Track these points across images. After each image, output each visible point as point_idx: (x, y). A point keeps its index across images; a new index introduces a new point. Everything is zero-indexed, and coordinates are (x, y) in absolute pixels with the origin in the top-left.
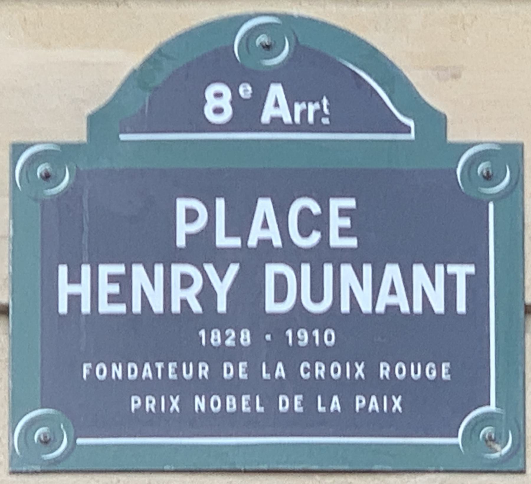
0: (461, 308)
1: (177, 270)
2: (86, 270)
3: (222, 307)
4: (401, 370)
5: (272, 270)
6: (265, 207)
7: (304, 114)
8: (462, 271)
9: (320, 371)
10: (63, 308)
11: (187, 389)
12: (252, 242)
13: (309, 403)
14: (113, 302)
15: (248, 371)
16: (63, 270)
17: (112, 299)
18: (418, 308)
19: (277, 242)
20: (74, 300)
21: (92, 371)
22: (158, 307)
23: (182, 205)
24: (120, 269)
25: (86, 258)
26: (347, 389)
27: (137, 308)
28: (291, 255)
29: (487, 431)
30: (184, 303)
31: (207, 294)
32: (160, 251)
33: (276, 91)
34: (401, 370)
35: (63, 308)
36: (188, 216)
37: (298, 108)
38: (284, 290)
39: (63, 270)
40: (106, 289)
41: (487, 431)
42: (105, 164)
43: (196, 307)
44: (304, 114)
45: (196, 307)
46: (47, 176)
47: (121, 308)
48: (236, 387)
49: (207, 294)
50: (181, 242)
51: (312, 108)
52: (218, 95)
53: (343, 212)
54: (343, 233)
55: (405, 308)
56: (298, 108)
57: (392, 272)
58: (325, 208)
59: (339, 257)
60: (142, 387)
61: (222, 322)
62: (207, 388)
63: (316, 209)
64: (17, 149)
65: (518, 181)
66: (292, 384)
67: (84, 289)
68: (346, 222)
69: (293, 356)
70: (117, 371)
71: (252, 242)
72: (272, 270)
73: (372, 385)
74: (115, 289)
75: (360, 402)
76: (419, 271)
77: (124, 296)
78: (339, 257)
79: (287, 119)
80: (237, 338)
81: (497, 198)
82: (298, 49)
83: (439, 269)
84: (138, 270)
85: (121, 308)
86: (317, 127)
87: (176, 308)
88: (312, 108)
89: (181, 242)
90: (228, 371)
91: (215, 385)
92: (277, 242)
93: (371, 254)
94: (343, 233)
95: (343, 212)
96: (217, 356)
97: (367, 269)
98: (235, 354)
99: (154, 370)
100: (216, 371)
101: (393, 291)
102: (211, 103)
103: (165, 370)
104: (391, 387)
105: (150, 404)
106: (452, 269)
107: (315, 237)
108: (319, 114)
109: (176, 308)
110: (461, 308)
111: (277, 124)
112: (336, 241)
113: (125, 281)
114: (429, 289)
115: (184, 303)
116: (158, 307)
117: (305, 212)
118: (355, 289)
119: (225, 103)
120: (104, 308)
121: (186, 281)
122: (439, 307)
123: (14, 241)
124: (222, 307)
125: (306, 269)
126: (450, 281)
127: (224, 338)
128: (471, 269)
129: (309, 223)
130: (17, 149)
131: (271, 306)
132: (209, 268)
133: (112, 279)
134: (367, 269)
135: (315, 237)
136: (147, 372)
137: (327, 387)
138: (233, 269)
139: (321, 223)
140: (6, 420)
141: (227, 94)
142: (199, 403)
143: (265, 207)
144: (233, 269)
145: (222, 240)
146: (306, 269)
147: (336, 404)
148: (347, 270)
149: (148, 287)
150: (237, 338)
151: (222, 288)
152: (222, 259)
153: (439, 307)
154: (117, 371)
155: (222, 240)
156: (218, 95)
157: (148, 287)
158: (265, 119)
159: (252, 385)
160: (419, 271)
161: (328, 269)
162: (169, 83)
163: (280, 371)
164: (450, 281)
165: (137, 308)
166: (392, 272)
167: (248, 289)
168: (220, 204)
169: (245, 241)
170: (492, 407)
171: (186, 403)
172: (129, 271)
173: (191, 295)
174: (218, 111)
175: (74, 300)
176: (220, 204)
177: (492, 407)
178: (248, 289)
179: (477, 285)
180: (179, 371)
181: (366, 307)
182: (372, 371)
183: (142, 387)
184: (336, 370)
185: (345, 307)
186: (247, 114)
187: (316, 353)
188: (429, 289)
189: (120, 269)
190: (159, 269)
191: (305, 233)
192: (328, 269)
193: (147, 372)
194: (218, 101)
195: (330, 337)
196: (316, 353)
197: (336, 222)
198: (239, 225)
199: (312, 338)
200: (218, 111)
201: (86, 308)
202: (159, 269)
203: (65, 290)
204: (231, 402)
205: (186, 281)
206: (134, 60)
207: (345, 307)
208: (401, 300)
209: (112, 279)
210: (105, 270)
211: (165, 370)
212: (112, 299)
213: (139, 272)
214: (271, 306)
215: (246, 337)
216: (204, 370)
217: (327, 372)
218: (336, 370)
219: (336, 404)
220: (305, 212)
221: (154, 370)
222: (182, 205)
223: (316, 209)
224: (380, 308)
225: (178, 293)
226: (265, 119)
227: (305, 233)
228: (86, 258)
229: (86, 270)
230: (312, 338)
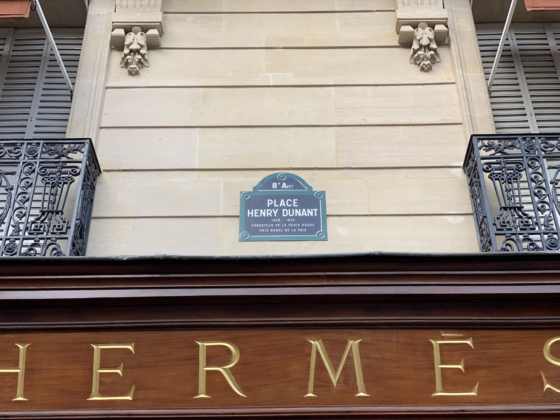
1: (268, 210)
3: (275, 215)
4: (306, 225)
5: (283, 210)
6: (282, 201)
8: (316, 210)
9: (292, 225)
11: (270, 228)
13: (290, 230)
17: (257, 214)
20: (250, 215)
23: (269, 200)
26: (297, 228)
31: (273, 214)
32: (265, 207)
33: (284, 184)
34: (306, 225)
36: (269, 202)
38: (286, 213)
40: (256, 213)
48: (278, 228)
49: (273, 214)
57: (304, 210)
59: (295, 208)
60: (262, 228)
61: (275, 218)
62: (273, 228)
64: (241, 192)
65: (325, 196)
66: (287, 227)
67: (252, 213)
69: (287, 223)
70: (258, 225)
72: (283, 210)
73: (301, 227)
76: (308, 210)
77: (259, 214)
78: (295, 208)
81: (321, 199)
82: (288, 178)
90: (276, 225)
91: (274, 227)
93: (300, 207)
96: (274, 223)
98: (278, 223)
100: (274, 225)
104: (304, 227)
105: (263, 231)
111: (284, 188)
112: (294, 205)
113: (259, 212)
116: (264, 216)
117: (289, 201)
118: (298, 213)
119: (276, 185)
120: (255, 216)
121: (269, 212)
122: (312, 215)
124: (275, 215)
125: (289, 210)
126: (314, 211)
129: (289, 203)
130: (241, 192)
131: (284, 215)
133: (257, 211)
137: (293, 228)
139: (292, 203)
142: (272, 230)
143: (282, 201)
145: (275, 205)
147: (295, 230)
148: (296, 210)
149: (263, 213)
151: (275, 213)
153: (312, 215)
154: (258, 225)
155: (275, 205)
157: (263, 213)
160: (308, 210)
162: (267, 183)
163: (285, 225)
164: (314, 211)
167: (280, 213)
171: (269, 230)
173: (270, 214)
175: (250, 215)
178: (280, 213)
179: (318, 212)
182: (301, 225)
183: (262, 228)
184: (295, 225)
186: (279, 187)
187: (291, 222)
188: (310, 212)
191: (289, 204)
194: (275, 185)
195: (294, 220)
196: (291, 222)
197: (294, 203)
198: (278, 203)
203: (249, 213)
204: (277, 230)
205: (269, 212)
206: (261, 179)
209: (257, 211)
210: (255, 210)
212: (257, 214)
214: (284, 215)
215: (279, 220)
218: (295, 225)
219: (295, 230)
220: (289, 201)
222: (269, 200)
227: (289, 204)
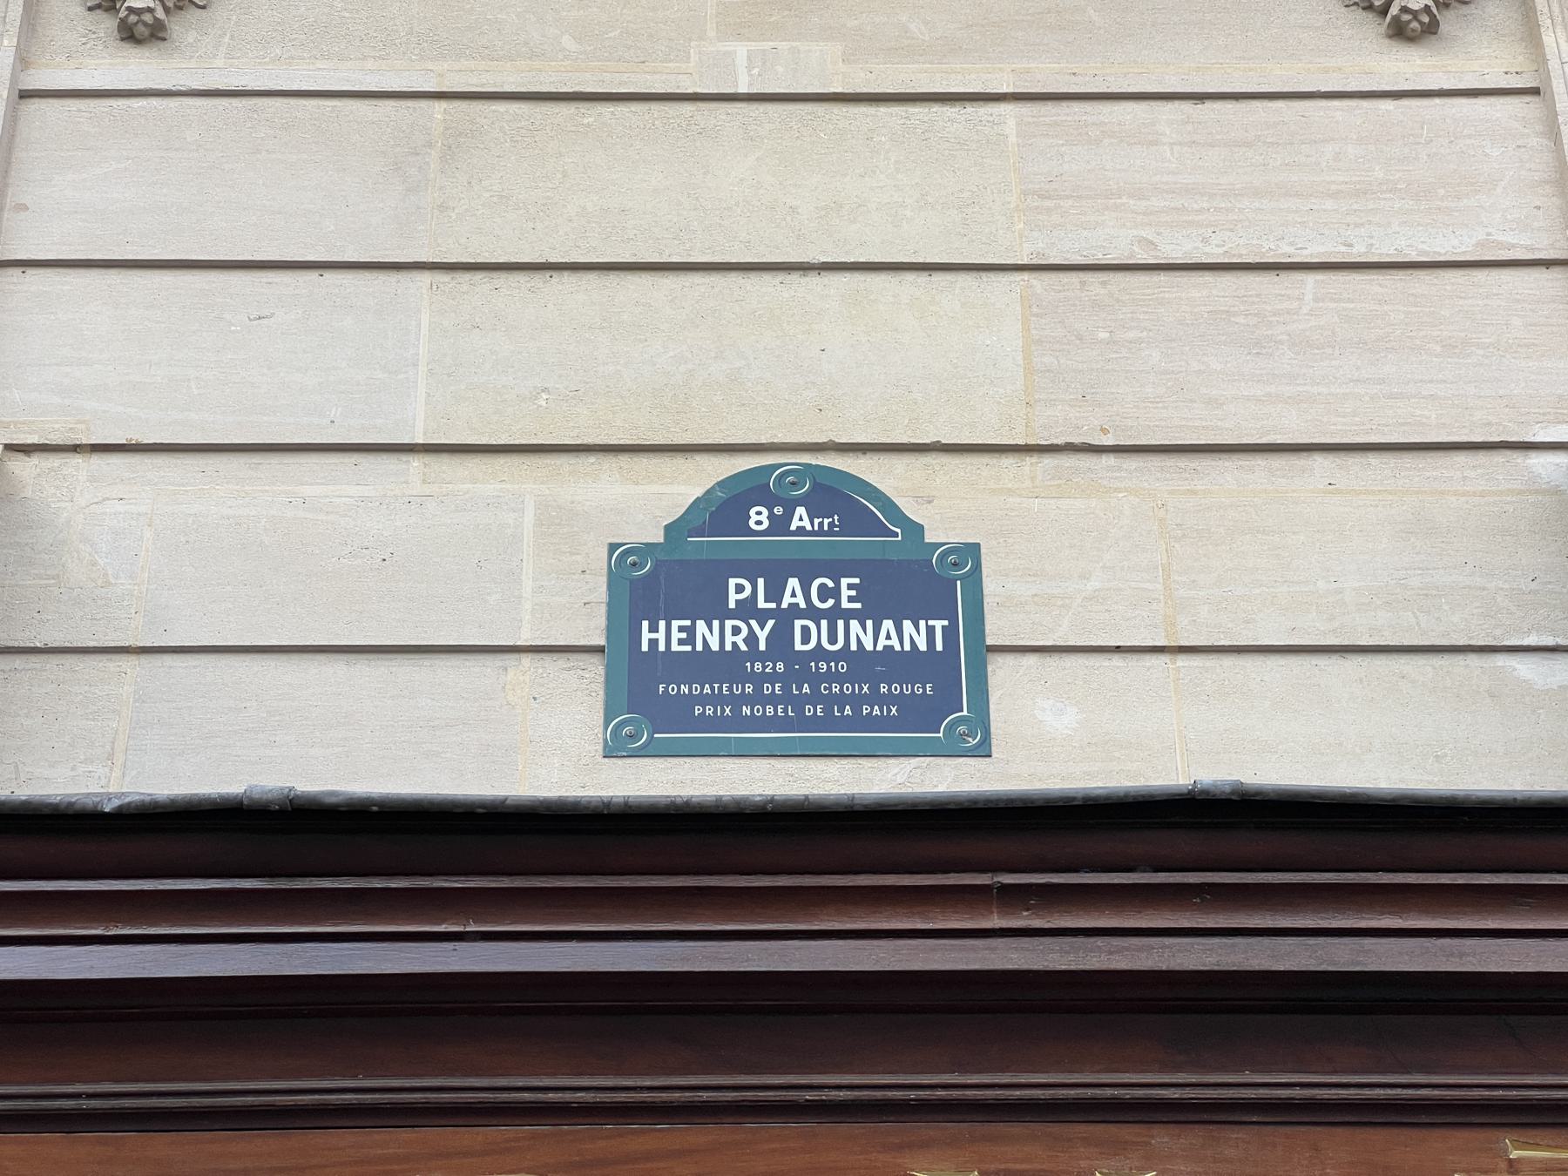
0: (939, 647)
1: (729, 624)
2: (662, 624)
3: (762, 647)
4: (896, 689)
5: (798, 624)
6: (793, 583)
7: (821, 524)
8: (939, 625)
9: (836, 689)
10: (645, 648)
11: (737, 701)
12: (784, 605)
13: (828, 711)
14: (675, 715)
15: (782, 689)
16: (645, 624)
17: (681, 642)
18: (907, 647)
19: (803, 605)
20: (653, 643)
21: (666, 689)
22: (715, 647)
23: (732, 582)
24: (688, 623)
25: (662, 614)
26: (857, 701)
27: (699, 647)
28: (813, 614)
29: (962, 729)
30: (734, 644)
31: (752, 639)
32: (716, 610)
33: (801, 511)
34: (896, 689)
35: (645, 648)
36: (736, 590)
37: (816, 521)
38: (809, 637)
39: (645, 624)
40: (676, 635)
41: (962, 729)
42: (677, 557)
43: (743, 647)
44: (821, 524)
45: (743, 647)
46: (634, 564)
47: (688, 648)
48: (773, 700)
49: (752, 639)
50: (732, 605)
51: (826, 521)
52: (759, 513)
53: (850, 587)
54: (851, 599)
55: (898, 648)
56: (816, 521)
57: (888, 625)
58: (838, 584)
59: (848, 615)
60: (703, 700)
61: (762, 657)
62: (751, 700)
63: (830, 584)
64: (613, 547)
65: (977, 567)
66: (815, 698)
67: (661, 636)
68: (853, 593)
69: (816, 679)
70: (685, 689)
71: (784, 605)
72: (798, 624)
73: (875, 698)
74: (684, 635)
75: (866, 710)
76: (907, 625)
77: (691, 640)
78: (848, 615)
79: (809, 528)
80: (774, 668)
81: (962, 578)
82: (816, 486)
83: (922, 623)
84: (701, 626)
85: (688, 648)
86: (830, 533)
87: (728, 647)
88: (826, 521)
89: (732, 605)
90: (767, 689)
91: (758, 698)
92: (803, 605)
93: (872, 612)
94: (851, 599)
95: (850, 587)
96: (759, 680)
97: (869, 623)
98: (773, 678)
99: (712, 689)
100: (758, 689)
101: (888, 637)
102: (754, 518)
103: (720, 689)
104: (888, 700)
105: (709, 711)
106: (931, 623)
107: (831, 602)
108: (831, 525)
109: (728, 647)
110: (939, 647)
111: (801, 531)
112: (845, 604)
113: (691, 631)
114: (915, 635)
115: (734, 644)
116: (715, 647)
117: (822, 587)
118: (861, 635)
119: (764, 517)
120: (675, 647)
121: (736, 631)
122: (923, 647)
123: (609, 605)
124: (762, 647)
125: (824, 623)
126: (931, 631)
127: (764, 667)
128: (946, 623)
129: (824, 593)
130: (613, 547)
131: (798, 646)
132: (753, 623)
133: (681, 629)
134: (869, 623)
135: (831, 602)
136: (707, 690)
137: (841, 700)
138: (771, 623)
139: (836, 594)
140: (601, 721)
141: (765, 512)
142: (746, 710)
143: (793, 583)
144: (771, 623)
145: (761, 604)
146: (824, 623)
147: (848, 711)
148: (854, 624)
149: (708, 635)
150: (774, 668)
151: (762, 635)
152: (762, 617)
153: (923, 647)
154: (685, 689)
155: (761, 604)
156: (759, 513)
157: (708, 635)
158: (793, 527)
159: (787, 698)
160: (907, 625)
161: (841, 623)
162: (723, 509)
163: (806, 689)
164: (931, 631)
165: (699, 647)
166: (888, 625)
167: (781, 637)
168: (761, 582)
169: (779, 603)
170: (965, 713)
171: (736, 711)
172: (694, 624)
173: (739, 639)
174: (759, 523)
175: (653, 643)
176: (761, 582)
177: (965, 713)
178: (781, 637)
179: (950, 634)
180: (730, 689)
181: (869, 647)
182: (875, 689)
183: (703, 700)
184: (848, 689)
185: (854, 647)
186: (779, 525)
187: (831, 677)
188: (915, 635)
189: (688, 623)
190: (716, 623)
191: (823, 600)
192: (841, 623)
193: (707, 690)
194: (759, 517)
195: (843, 667)
196: (831, 677)
197: (845, 593)
198: (775, 593)
199: (829, 668)
200: (759, 523)
201: (662, 647)
202: (716, 623)
203: (646, 636)
204: (770, 710)
205: (736, 631)
206: (699, 492)
207: (854, 647)
208: (895, 642)
209: (681, 629)
210: (675, 624)
211: (720, 689)
212: (681, 642)
213: (701, 626)
214: (798, 646)
215: (780, 667)
216: (749, 689)
217: (841, 690)
218: (848, 689)
219: (848, 711)
220: (822, 587)
221: (712, 689)
222: (732, 582)
223: (830, 584)
224: (880, 648)
225: (729, 639)
226: (793, 527)
227: (823, 600)
228: (662, 614)
229: (662, 624)
230: (829, 668)
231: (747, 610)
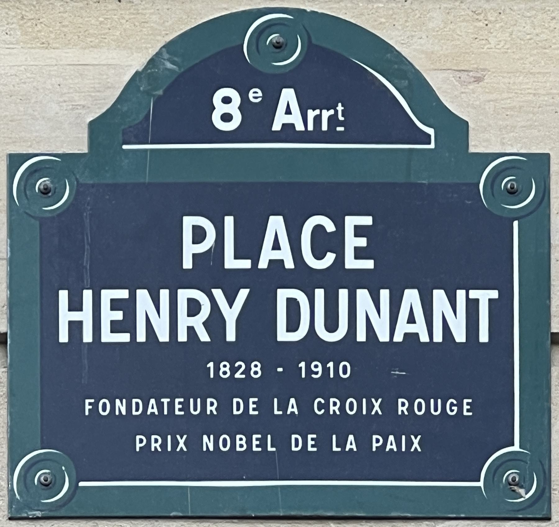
0: (484, 337)
1: (184, 295)
2: (88, 295)
3: (231, 336)
5: (283, 295)
6: (276, 224)
7: (318, 120)
8: (485, 296)
10: (64, 337)
12: (263, 264)
13: (323, 443)
16: (63, 295)
17: (116, 327)
18: (438, 337)
19: (289, 264)
20: (75, 327)
21: (95, 405)
22: (163, 336)
24: (124, 294)
25: (87, 280)
26: (363, 426)
27: (141, 337)
28: (304, 278)
30: (191, 330)
31: (216, 322)
32: (165, 274)
33: (288, 96)
35: (64, 337)
36: (196, 236)
37: (311, 114)
39: (63, 295)
40: (109, 316)
44: (318, 120)
45: (204, 337)
46: (46, 191)
47: (125, 338)
48: (245, 425)
49: (216, 322)
50: (188, 264)
51: (326, 114)
52: (227, 100)
53: (359, 231)
54: (359, 253)
55: (424, 338)
56: (311, 114)
61: (231, 353)
63: (330, 227)
64: (15, 160)
66: (305, 422)
67: (85, 316)
69: (307, 390)
70: (121, 407)
71: (263, 264)
72: (283, 295)
73: (391, 423)
74: (118, 315)
76: (439, 296)
77: (126, 325)
79: (300, 127)
82: (311, 49)
83: (461, 294)
84: (143, 295)
85: (125, 338)
86: (330, 136)
87: (182, 337)
88: (326, 114)
89: (188, 264)
91: (224, 423)
92: (289, 264)
93: (388, 278)
94: (359, 253)
95: (359, 231)
96: (226, 390)
97: (385, 294)
98: (245, 388)
100: (225, 406)
101: (411, 320)
102: (220, 109)
103: (171, 405)
106: (474, 294)
107: (330, 258)
108: (332, 120)
109: (182, 337)
111: (288, 132)
112: (351, 263)
113: (127, 307)
115: (191, 330)
116: (163, 336)
117: (318, 229)
118: (373, 316)
119: (233, 109)
120: (107, 337)
121: (194, 308)
122: (460, 336)
123: (12, 262)
124: (231, 336)
125: (320, 294)
126: (472, 306)
127: (234, 370)
129: (324, 242)
130: (15, 160)
131: (283, 335)
132: (218, 294)
133: (115, 304)
134: (385, 294)
135: (330, 258)
137: (342, 425)
142: (208, 443)
143: (276, 224)
145: (231, 263)
146: (320, 294)
147: (351, 444)
148: (363, 295)
149: (154, 315)
151: (231, 315)
152: (231, 283)
153: (460, 336)
154: (121, 407)
155: (231, 263)
157: (154, 315)
158: (277, 127)
159: (263, 423)
160: (439, 296)
161: (343, 294)
163: (293, 407)
164: (472, 306)
165: (141, 337)
167: (258, 317)
168: (229, 221)
169: (255, 263)
170: (516, 447)
172: (133, 296)
174: (227, 118)
175: (75, 327)
176: (229, 221)
177: (516, 447)
178: (258, 317)
179: (500, 311)
180: (185, 407)
181: (383, 336)
183: (148, 425)
185: (361, 336)
186: (257, 121)
189: (124, 294)
190: (164, 294)
191: (319, 255)
192: (343, 294)
193: (152, 409)
194: (226, 107)
197: (352, 242)
199: (326, 370)
200: (227, 118)
201: (88, 337)
202: (164, 294)
203: (65, 316)
204: (241, 441)
205: (194, 308)
206: (137, 62)
207: (361, 336)
208: (420, 328)
209: (115, 304)
210: (107, 295)
211: (171, 405)
212: (116, 327)
214: (283, 335)
215: (256, 369)
219: (351, 444)
220: (318, 229)
221: (160, 406)
223: (330, 227)
224: (398, 338)
225: (184, 321)
226: (277, 127)
227: (319, 255)
228: (87, 280)
229: (88, 295)
230: (326, 370)
231: (209, 273)
